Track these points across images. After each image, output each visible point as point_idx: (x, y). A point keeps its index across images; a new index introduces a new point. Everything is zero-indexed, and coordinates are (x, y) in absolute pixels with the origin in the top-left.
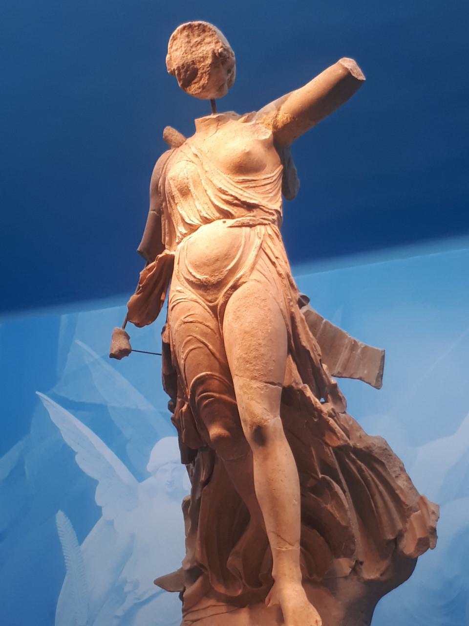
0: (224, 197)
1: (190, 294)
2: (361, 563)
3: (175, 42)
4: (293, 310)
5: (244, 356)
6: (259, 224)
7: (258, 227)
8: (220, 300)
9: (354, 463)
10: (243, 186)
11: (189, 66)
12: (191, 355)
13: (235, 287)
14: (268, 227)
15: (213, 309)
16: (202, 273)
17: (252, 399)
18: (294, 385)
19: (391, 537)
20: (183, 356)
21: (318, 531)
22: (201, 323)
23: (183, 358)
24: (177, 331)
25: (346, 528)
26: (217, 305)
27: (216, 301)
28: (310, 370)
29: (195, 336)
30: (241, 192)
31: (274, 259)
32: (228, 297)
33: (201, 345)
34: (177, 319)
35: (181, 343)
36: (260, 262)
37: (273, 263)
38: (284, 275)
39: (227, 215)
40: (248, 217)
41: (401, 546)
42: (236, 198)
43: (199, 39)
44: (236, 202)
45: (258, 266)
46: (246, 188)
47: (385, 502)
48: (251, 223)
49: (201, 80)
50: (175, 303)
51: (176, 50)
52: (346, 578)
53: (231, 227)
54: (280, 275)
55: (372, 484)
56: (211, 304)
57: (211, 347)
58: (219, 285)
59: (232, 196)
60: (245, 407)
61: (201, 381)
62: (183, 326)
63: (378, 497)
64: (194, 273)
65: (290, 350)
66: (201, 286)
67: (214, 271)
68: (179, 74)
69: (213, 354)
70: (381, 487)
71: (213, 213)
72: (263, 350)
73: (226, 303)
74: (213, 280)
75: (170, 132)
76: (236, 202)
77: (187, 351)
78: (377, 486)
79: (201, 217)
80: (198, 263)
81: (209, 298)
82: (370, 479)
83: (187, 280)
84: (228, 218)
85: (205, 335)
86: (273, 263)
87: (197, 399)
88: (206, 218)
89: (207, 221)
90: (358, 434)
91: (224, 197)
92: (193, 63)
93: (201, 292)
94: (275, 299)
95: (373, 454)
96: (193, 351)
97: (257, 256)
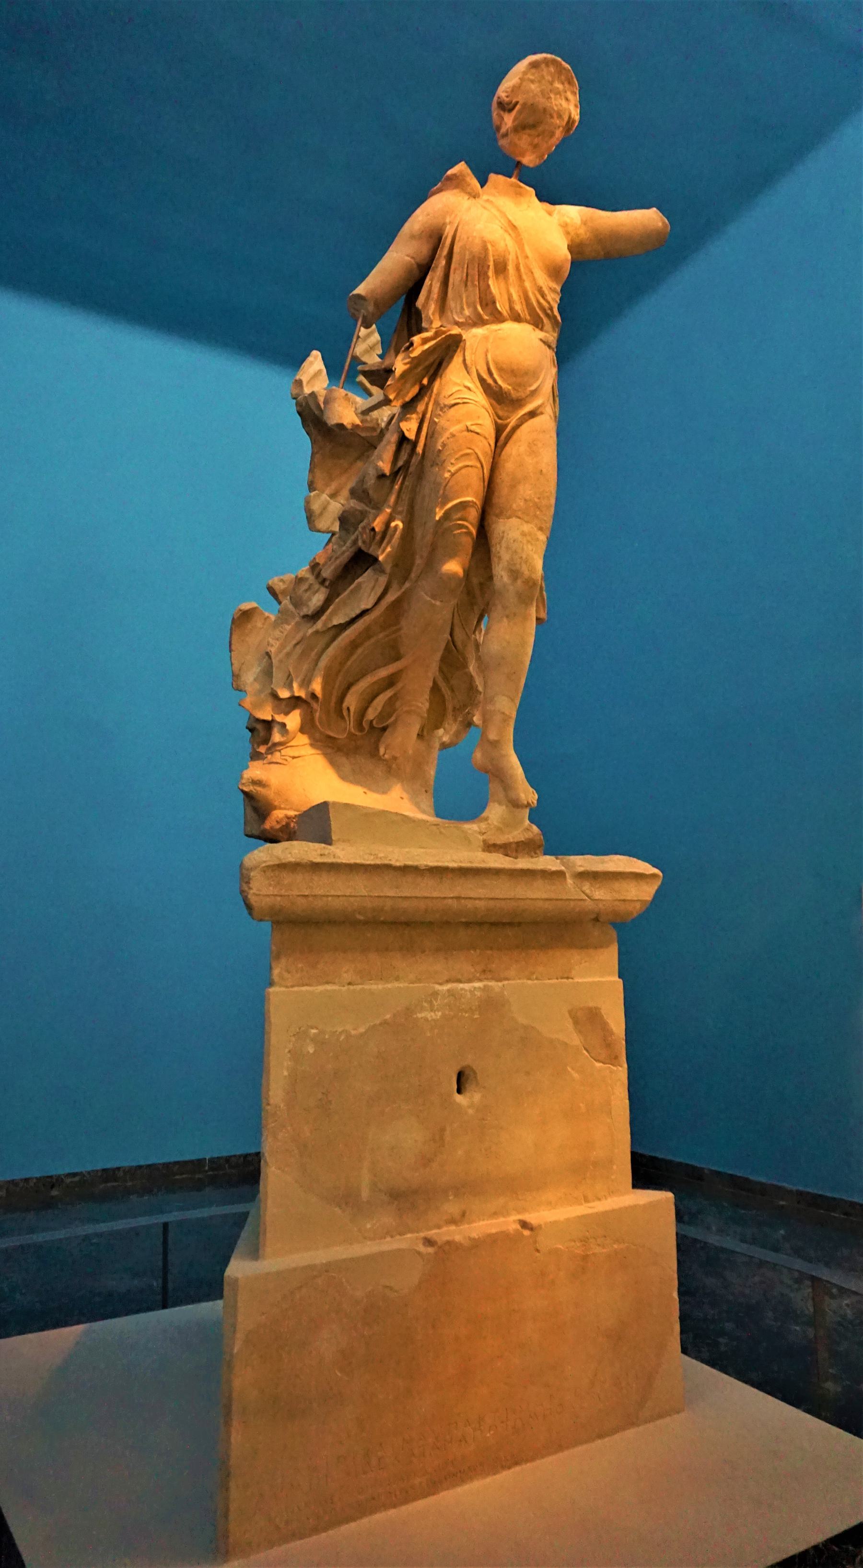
0: (542, 301)
3: (533, 71)
5: (536, 500)
8: (513, 421)
12: (463, 471)
13: (532, 414)
15: (499, 430)
16: (504, 380)
17: (535, 553)
20: (453, 469)
22: (485, 438)
23: (449, 471)
24: (453, 436)
26: (506, 426)
27: (508, 417)
29: (477, 451)
33: (479, 465)
34: (459, 422)
35: (455, 453)
39: (537, 323)
42: (551, 309)
43: (558, 85)
44: (549, 312)
49: (538, 136)
51: (532, 81)
53: (541, 340)
56: (499, 421)
57: (485, 471)
59: (548, 303)
60: (524, 557)
61: (463, 506)
62: (466, 433)
64: (496, 376)
67: (520, 385)
76: (549, 312)
77: (460, 465)
79: (511, 308)
80: (504, 366)
81: (500, 413)
83: (482, 381)
84: (537, 327)
88: (519, 315)
89: (517, 318)
91: (542, 301)
93: (494, 402)
96: (470, 469)
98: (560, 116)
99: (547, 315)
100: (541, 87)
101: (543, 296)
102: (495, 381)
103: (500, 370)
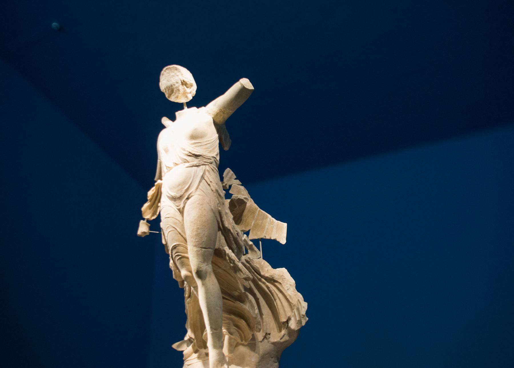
2: (269, 334)
4: (220, 209)
6: (203, 165)
7: (201, 166)
9: (264, 283)
10: (194, 145)
11: (169, 87)
13: (188, 199)
14: (207, 166)
18: (221, 247)
19: (284, 320)
21: (244, 320)
25: (256, 318)
27: (180, 205)
28: (232, 239)
30: (193, 149)
31: (209, 183)
32: (185, 204)
33: (174, 229)
36: (201, 184)
37: (209, 185)
38: (214, 191)
39: (186, 161)
40: (196, 161)
41: (289, 325)
42: (190, 153)
43: (173, 74)
44: (190, 154)
45: (200, 187)
46: (196, 146)
47: (281, 302)
48: (197, 165)
52: (261, 342)
54: (213, 191)
55: (275, 294)
57: (178, 230)
58: (180, 198)
61: (175, 247)
63: (278, 300)
65: (219, 229)
66: (174, 199)
67: (178, 190)
68: (166, 92)
69: (180, 234)
70: (280, 295)
71: (179, 161)
72: (199, 231)
73: (184, 207)
74: (178, 195)
75: (165, 121)
78: (277, 295)
81: (177, 205)
82: (273, 291)
85: (175, 224)
86: (209, 185)
87: (174, 256)
89: (176, 164)
90: (266, 269)
92: (172, 86)
94: (208, 203)
95: (275, 279)
97: (200, 182)
98: (177, 83)
101: (184, 150)
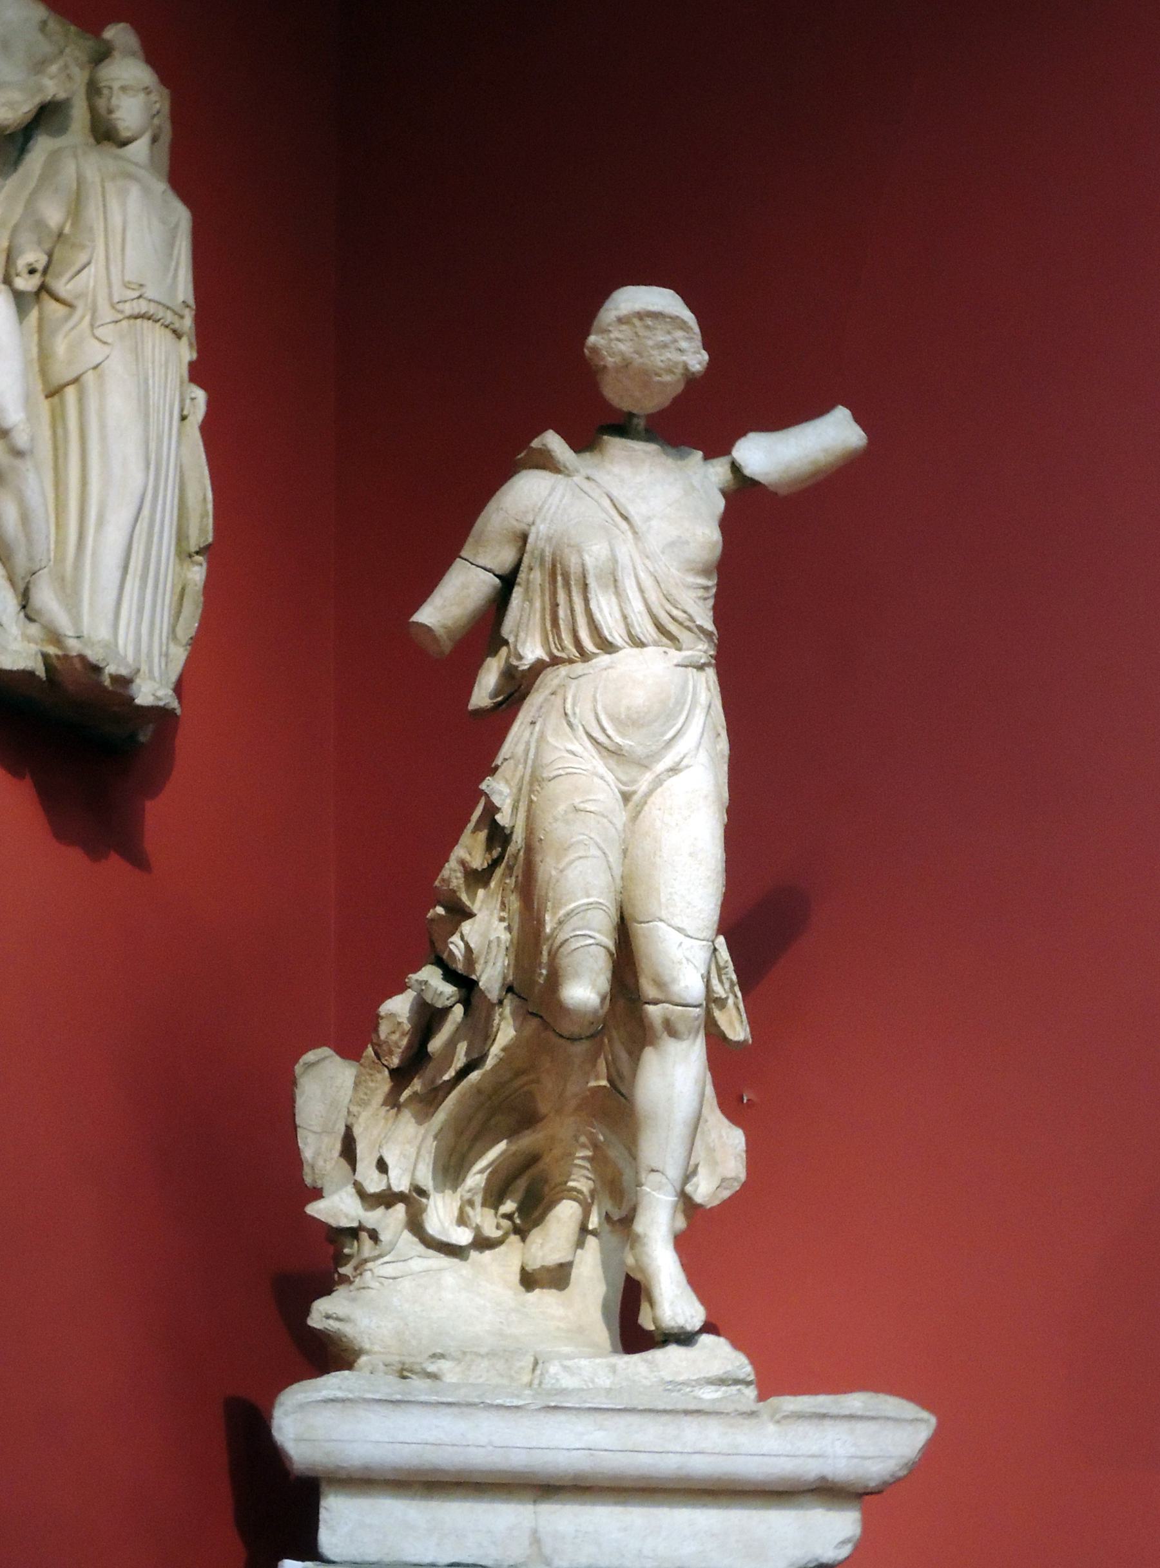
1: (593, 761)
13: (674, 770)
15: (626, 797)
16: (623, 735)
26: (634, 792)
27: (634, 781)
29: (592, 835)
32: (658, 782)
33: (599, 853)
42: (692, 619)
50: (561, 772)
53: (677, 665)
57: (611, 859)
64: (610, 732)
81: (624, 778)
89: (637, 643)
91: (675, 612)
99: (689, 629)
100: (649, 329)
102: (609, 737)
103: (613, 719)
